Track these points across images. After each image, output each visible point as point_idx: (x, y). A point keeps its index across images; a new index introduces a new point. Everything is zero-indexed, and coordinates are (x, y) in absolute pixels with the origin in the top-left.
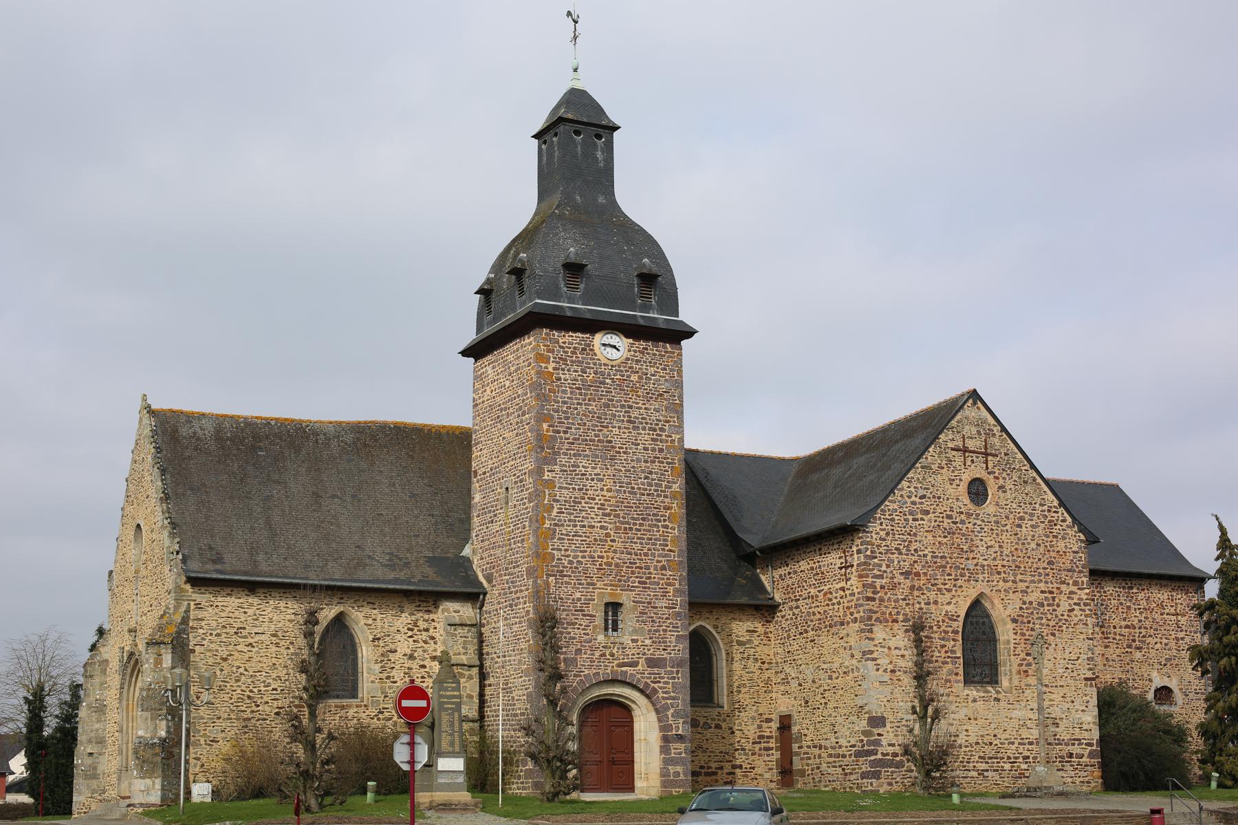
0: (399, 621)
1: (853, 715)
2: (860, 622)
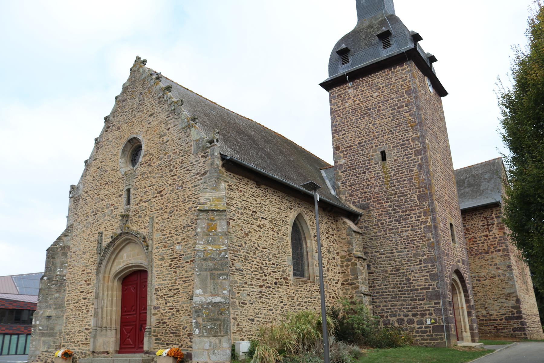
0: (322, 226)
1: (502, 298)
2: (503, 251)
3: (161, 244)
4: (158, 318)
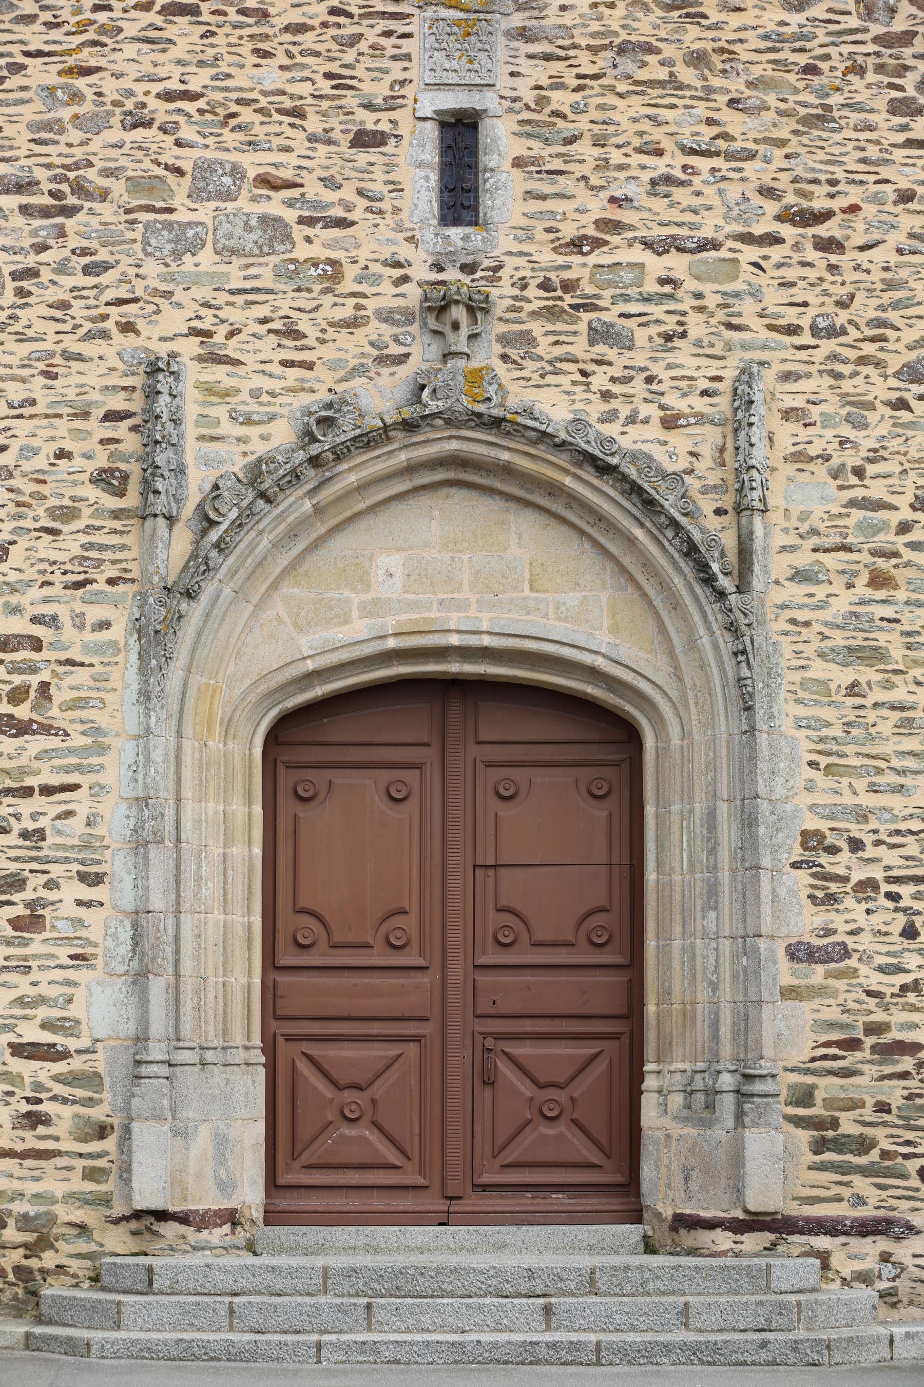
3: (843, 556)
4: (833, 1014)
